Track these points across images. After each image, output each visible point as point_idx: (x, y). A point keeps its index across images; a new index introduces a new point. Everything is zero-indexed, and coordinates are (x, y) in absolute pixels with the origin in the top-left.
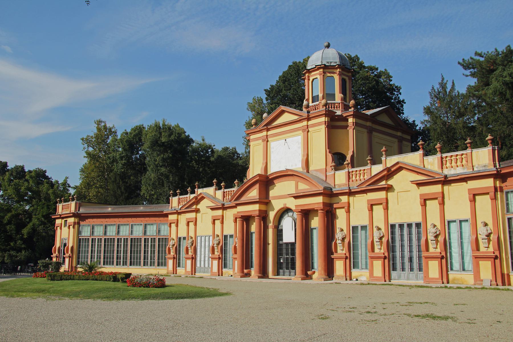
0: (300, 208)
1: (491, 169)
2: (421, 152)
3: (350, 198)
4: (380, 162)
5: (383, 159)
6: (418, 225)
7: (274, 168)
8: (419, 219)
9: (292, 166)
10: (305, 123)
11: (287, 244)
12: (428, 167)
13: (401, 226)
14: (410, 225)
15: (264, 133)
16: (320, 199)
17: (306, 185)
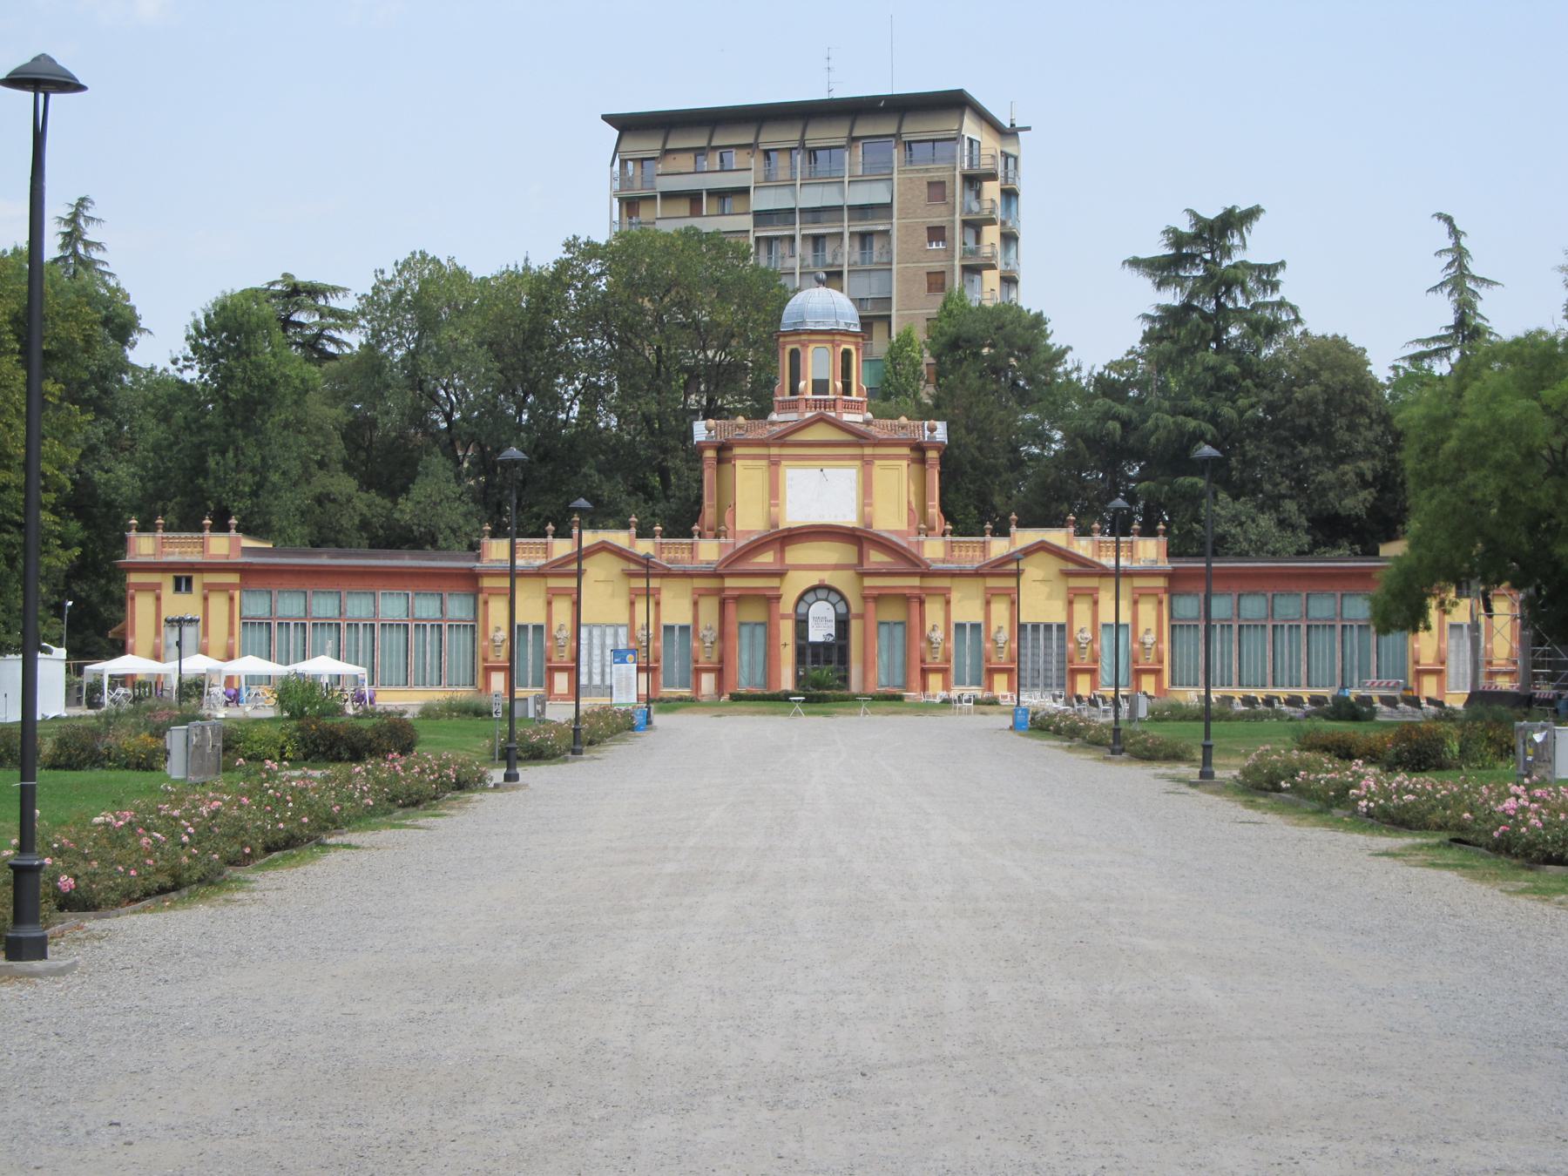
0: (876, 592)
1: (1165, 565)
2: (1071, 529)
3: (1277, 600)
4: (1006, 533)
5: (1013, 529)
6: (1061, 627)
7: (795, 515)
8: (1062, 619)
9: (836, 517)
10: (868, 451)
11: (816, 645)
12: (1081, 552)
13: (1036, 627)
14: (1048, 627)
15: (774, 451)
16: (916, 582)
17: (889, 556)
